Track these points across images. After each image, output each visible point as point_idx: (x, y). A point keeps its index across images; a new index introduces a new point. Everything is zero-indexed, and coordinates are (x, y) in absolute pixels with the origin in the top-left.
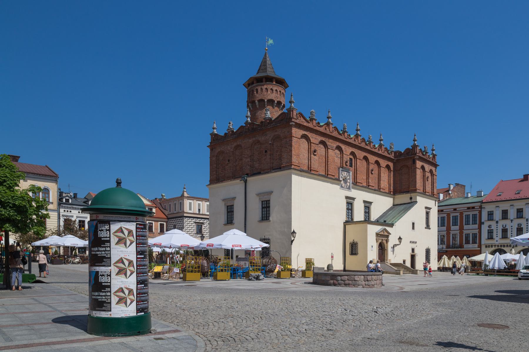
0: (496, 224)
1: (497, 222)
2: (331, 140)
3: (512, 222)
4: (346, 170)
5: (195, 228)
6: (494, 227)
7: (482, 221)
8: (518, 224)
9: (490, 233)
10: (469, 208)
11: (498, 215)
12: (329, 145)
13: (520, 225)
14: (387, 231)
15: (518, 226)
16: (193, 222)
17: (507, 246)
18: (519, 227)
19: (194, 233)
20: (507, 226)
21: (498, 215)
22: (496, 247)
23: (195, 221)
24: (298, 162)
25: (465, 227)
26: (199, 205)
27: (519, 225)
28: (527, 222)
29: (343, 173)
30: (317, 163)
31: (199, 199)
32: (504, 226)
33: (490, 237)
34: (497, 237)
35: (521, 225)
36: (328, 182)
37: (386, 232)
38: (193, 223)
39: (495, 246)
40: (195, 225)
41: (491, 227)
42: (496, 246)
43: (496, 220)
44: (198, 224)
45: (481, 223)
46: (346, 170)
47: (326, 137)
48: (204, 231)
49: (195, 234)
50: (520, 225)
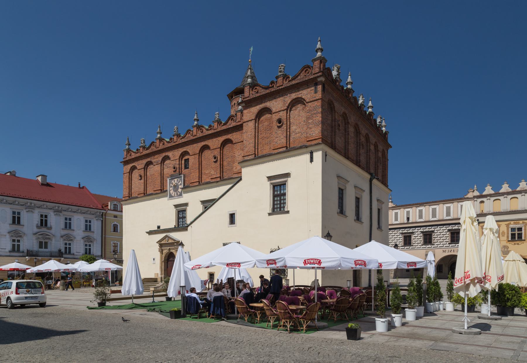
2: (156, 156)
4: (176, 177)
5: (401, 240)
12: (155, 162)
14: (160, 240)
16: (399, 233)
19: (401, 245)
23: (401, 232)
24: (127, 193)
26: (408, 213)
29: (173, 181)
30: (138, 185)
31: (447, 201)
36: (153, 199)
37: (162, 241)
38: (399, 234)
40: (401, 236)
44: (405, 235)
46: (176, 177)
47: (151, 156)
48: (414, 241)
49: (402, 246)
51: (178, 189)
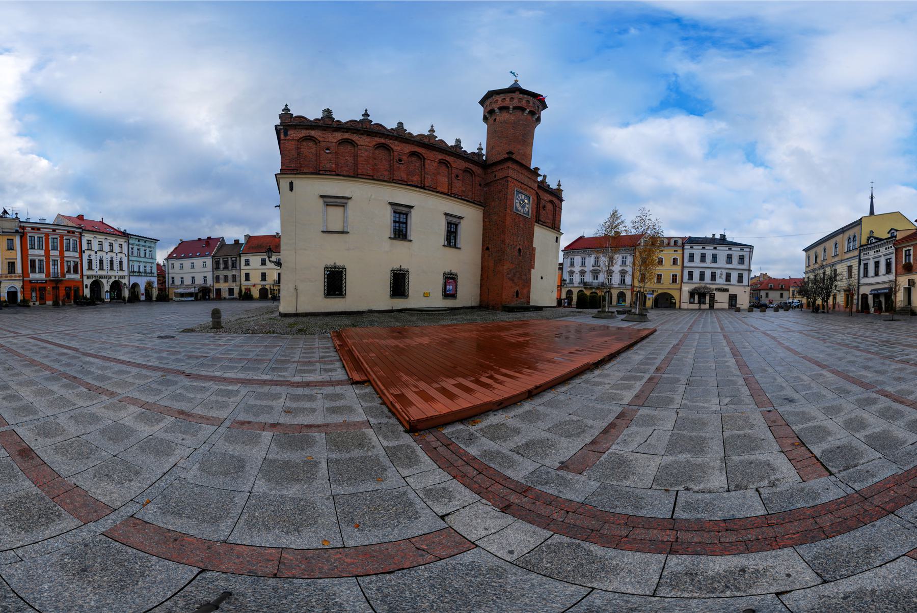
1: (96, 253)
6: (93, 258)
9: (90, 262)
10: (69, 232)
11: (95, 246)
13: (112, 258)
21: (95, 246)
25: (66, 254)
33: (90, 268)
45: (82, 252)
50: (112, 258)
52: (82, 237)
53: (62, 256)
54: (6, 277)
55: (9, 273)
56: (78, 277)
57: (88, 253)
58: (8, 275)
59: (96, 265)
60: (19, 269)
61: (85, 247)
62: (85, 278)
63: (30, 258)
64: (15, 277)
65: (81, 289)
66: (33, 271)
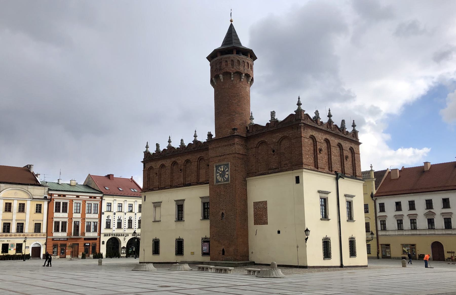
0: (114, 215)
1: (115, 214)
3: (125, 215)
7: (103, 211)
8: (130, 217)
10: (91, 197)
11: (115, 208)
15: (130, 219)
17: (122, 235)
18: (130, 219)
20: (121, 217)
21: (115, 208)
22: (113, 235)
25: (87, 216)
27: (130, 218)
28: (136, 216)
32: (120, 218)
33: (108, 226)
34: (114, 226)
35: (131, 218)
39: (112, 235)
41: (109, 218)
42: (113, 235)
43: (114, 212)
45: (101, 213)
51: (225, 175)
52: (103, 201)
53: (83, 218)
54: (32, 235)
55: (35, 232)
56: (95, 235)
57: (106, 214)
58: (34, 234)
59: (114, 225)
60: (44, 229)
61: (104, 208)
62: (102, 236)
63: (55, 220)
64: (40, 235)
65: (98, 245)
66: (57, 230)
